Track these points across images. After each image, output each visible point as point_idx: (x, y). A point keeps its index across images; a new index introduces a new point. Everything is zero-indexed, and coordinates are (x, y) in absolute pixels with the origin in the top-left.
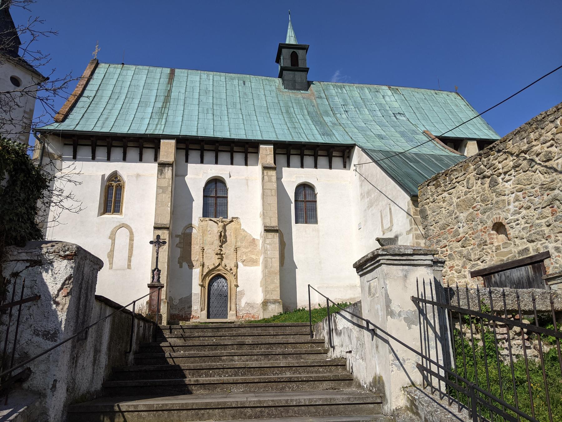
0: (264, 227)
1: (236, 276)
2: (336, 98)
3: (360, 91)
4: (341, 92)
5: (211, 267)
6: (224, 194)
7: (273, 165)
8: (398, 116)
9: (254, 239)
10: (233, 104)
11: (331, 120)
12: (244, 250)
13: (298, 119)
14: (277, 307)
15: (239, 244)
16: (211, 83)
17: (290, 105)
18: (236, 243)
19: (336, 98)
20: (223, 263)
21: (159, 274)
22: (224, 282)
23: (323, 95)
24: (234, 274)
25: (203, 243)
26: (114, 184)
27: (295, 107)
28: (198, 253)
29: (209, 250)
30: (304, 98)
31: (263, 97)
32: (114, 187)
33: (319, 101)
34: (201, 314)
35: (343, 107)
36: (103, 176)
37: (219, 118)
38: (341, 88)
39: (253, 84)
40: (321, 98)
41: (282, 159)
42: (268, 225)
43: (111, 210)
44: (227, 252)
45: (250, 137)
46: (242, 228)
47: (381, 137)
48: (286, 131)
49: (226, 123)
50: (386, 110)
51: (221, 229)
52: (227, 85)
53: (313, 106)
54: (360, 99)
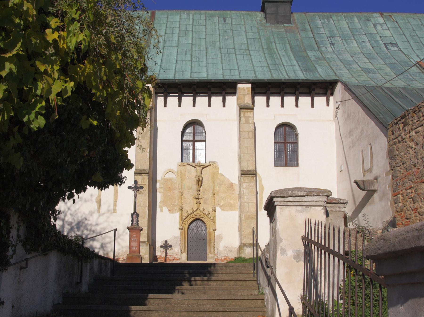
0: (241, 171)
1: (214, 220)
2: (322, 30)
3: (348, 20)
4: (327, 23)
5: (190, 212)
7: (251, 105)
8: (390, 47)
9: (232, 184)
10: (213, 43)
11: (315, 54)
13: (279, 55)
15: (217, 188)
16: (191, 22)
17: (272, 40)
19: (322, 30)
20: (202, 206)
21: (138, 218)
23: (308, 27)
24: (212, 218)
25: (182, 188)
27: (277, 42)
30: (286, 32)
31: (244, 34)
33: (303, 34)
34: (181, 256)
35: (329, 39)
37: (198, 59)
38: (328, 20)
39: (234, 20)
40: (305, 30)
41: (260, 100)
42: (245, 169)
44: (206, 196)
45: (229, 76)
46: (220, 172)
47: (367, 71)
48: (266, 69)
49: (204, 64)
50: (376, 41)
51: (199, 174)
52: (207, 23)
53: (297, 40)
54: (348, 29)
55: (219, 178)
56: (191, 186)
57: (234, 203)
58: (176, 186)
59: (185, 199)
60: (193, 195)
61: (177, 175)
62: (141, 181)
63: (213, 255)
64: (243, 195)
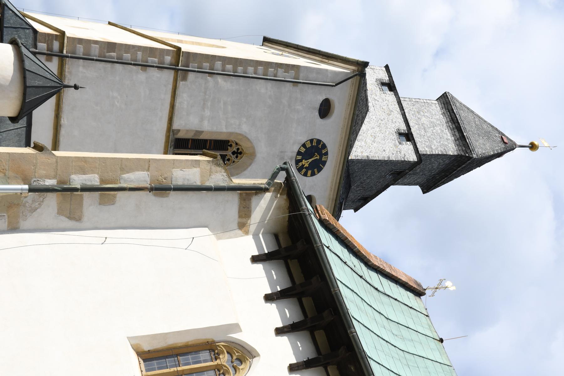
26: (224, 359)
32: (218, 362)
36: (236, 327)
43: (153, 369)
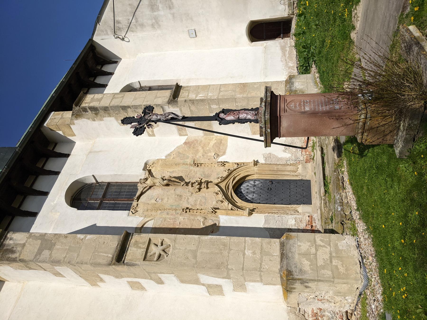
5: (221, 196)
6: (102, 188)
9: (185, 143)
12: (200, 154)
14: (298, 80)
15: (189, 161)
18: (187, 164)
22: (247, 184)
25: (176, 210)
28: (192, 218)
29: (190, 200)
46: (164, 158)
55: (173, 158)
56: (176, 196)
57: (216, 140)
58: (170, 219)
59: (196, 205)
60: (192, 193)
61: (149, 217)
62: (140, 248)
63: (300, 166)
64: (207, 97)
